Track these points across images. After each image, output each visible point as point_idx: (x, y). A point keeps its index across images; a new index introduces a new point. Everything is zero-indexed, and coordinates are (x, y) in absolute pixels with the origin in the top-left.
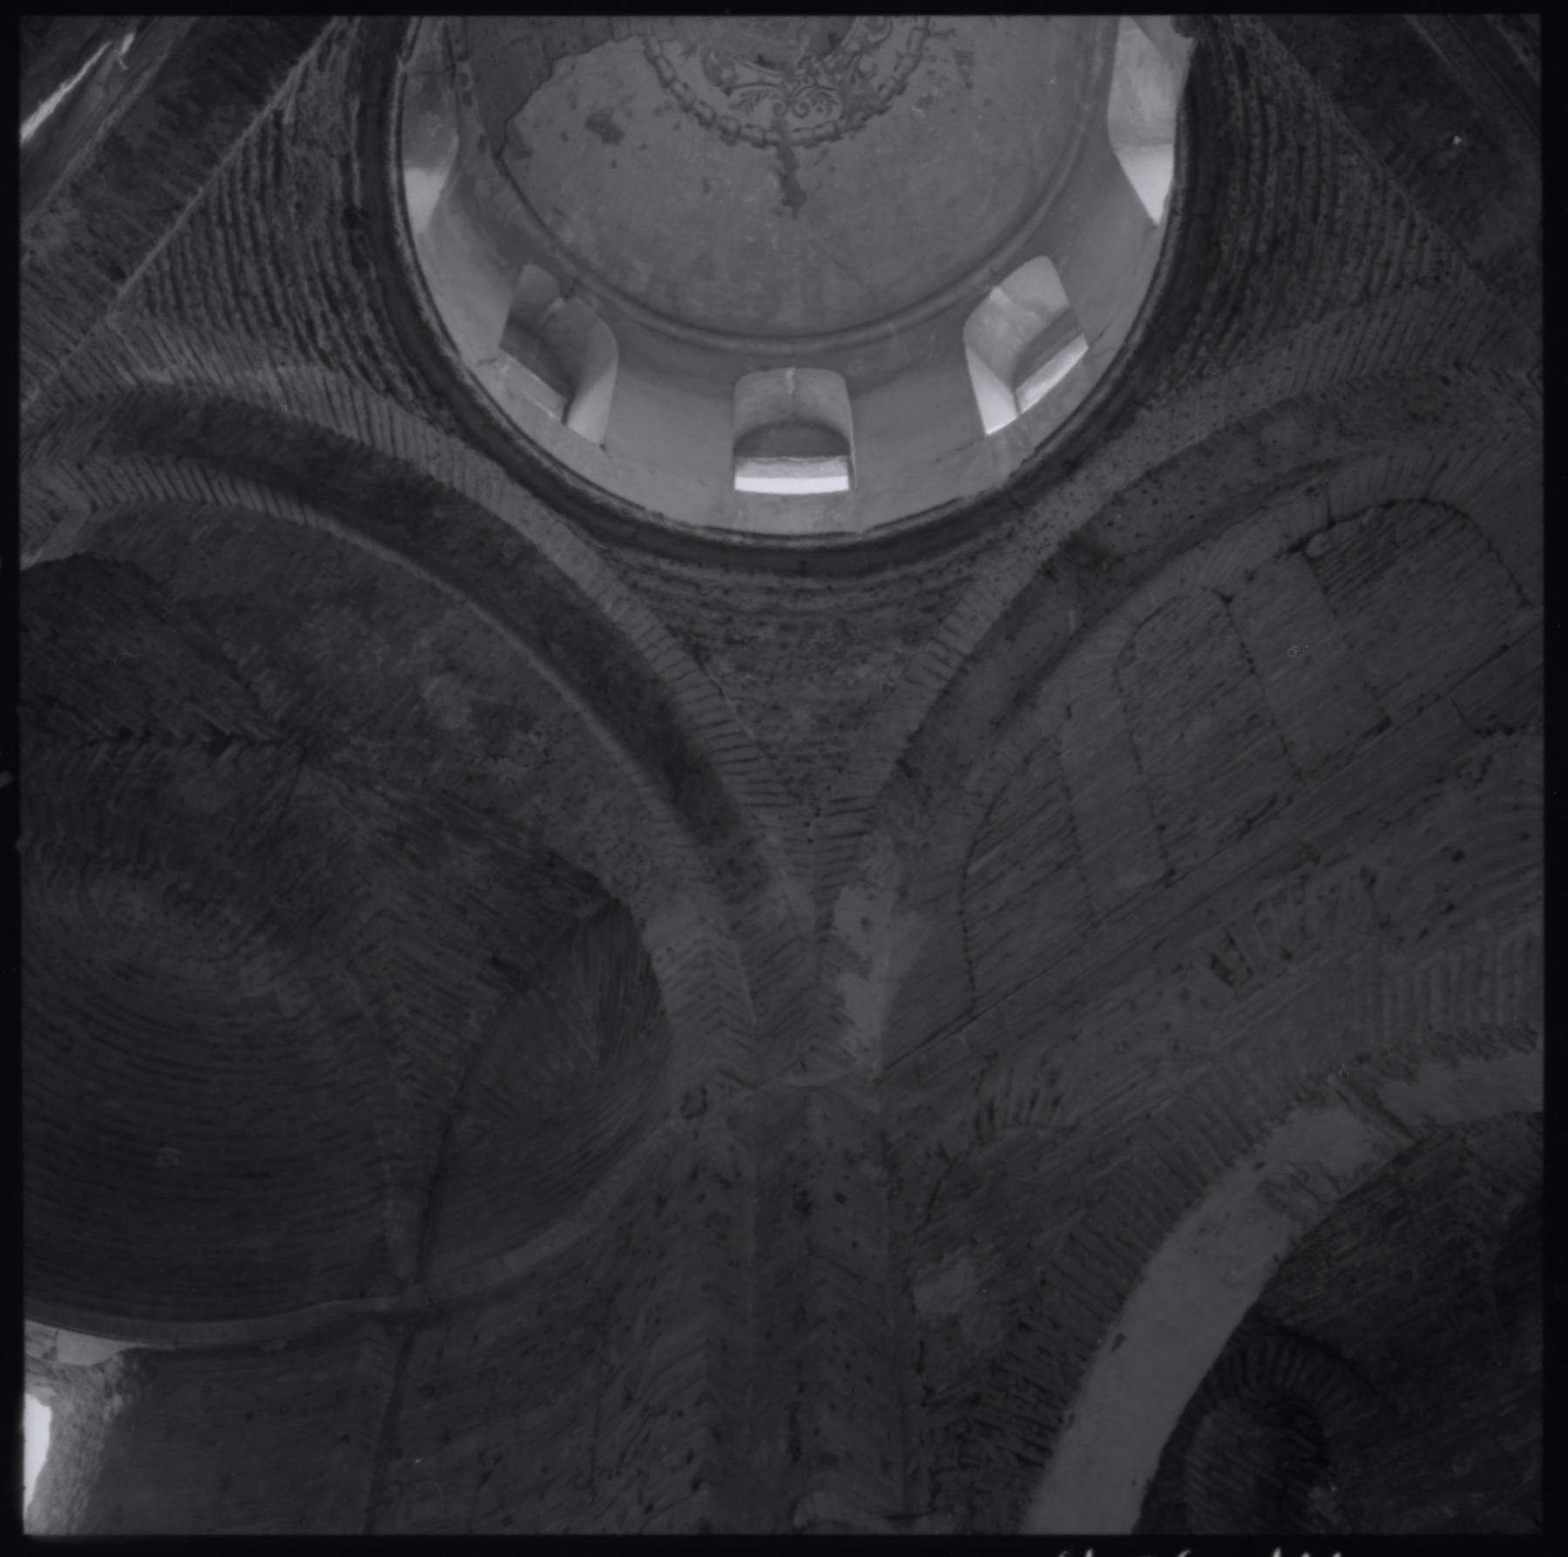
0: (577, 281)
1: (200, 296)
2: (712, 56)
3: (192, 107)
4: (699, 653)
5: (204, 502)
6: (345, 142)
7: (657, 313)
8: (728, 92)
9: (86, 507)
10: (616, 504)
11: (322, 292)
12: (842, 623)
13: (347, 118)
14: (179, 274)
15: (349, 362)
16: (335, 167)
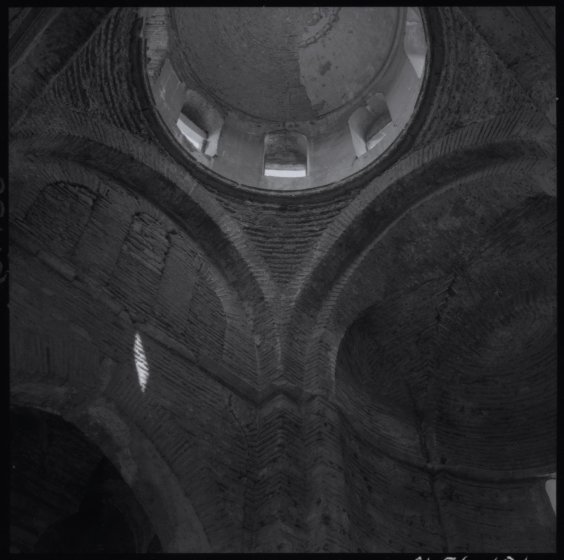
0: (363, 98)
1: (290, 265)
2: (309, 22)
3: (229, 260)
4: (458, 126)
5: (343, 290)
6: (259, 208)
7: (381, 69)
8: (321, 17)
9: (323, 330)
10: (399, 140)
11: (302, 224)
12: (460, 65)
13: (251, 206)
14: (281, 270)
15: (326, 221)
16: (266, 212)
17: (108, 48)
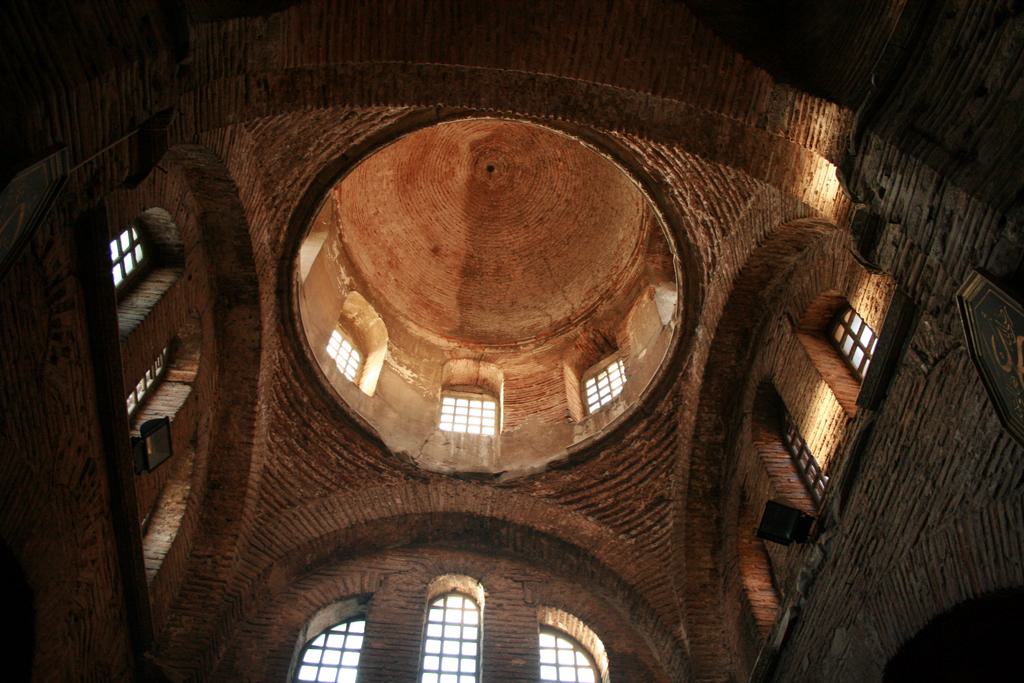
17: (594, 490)
